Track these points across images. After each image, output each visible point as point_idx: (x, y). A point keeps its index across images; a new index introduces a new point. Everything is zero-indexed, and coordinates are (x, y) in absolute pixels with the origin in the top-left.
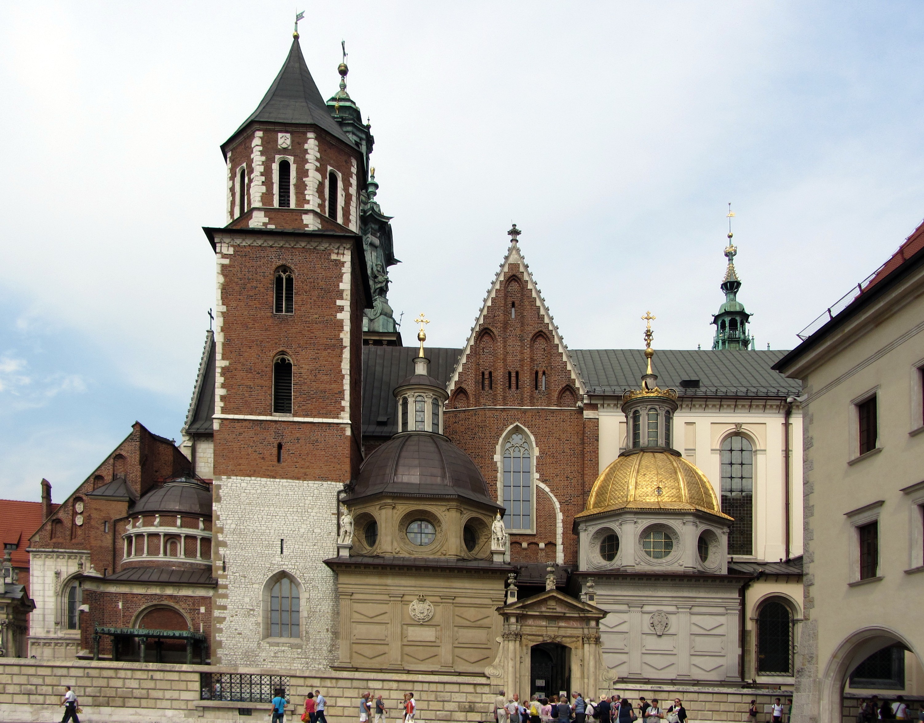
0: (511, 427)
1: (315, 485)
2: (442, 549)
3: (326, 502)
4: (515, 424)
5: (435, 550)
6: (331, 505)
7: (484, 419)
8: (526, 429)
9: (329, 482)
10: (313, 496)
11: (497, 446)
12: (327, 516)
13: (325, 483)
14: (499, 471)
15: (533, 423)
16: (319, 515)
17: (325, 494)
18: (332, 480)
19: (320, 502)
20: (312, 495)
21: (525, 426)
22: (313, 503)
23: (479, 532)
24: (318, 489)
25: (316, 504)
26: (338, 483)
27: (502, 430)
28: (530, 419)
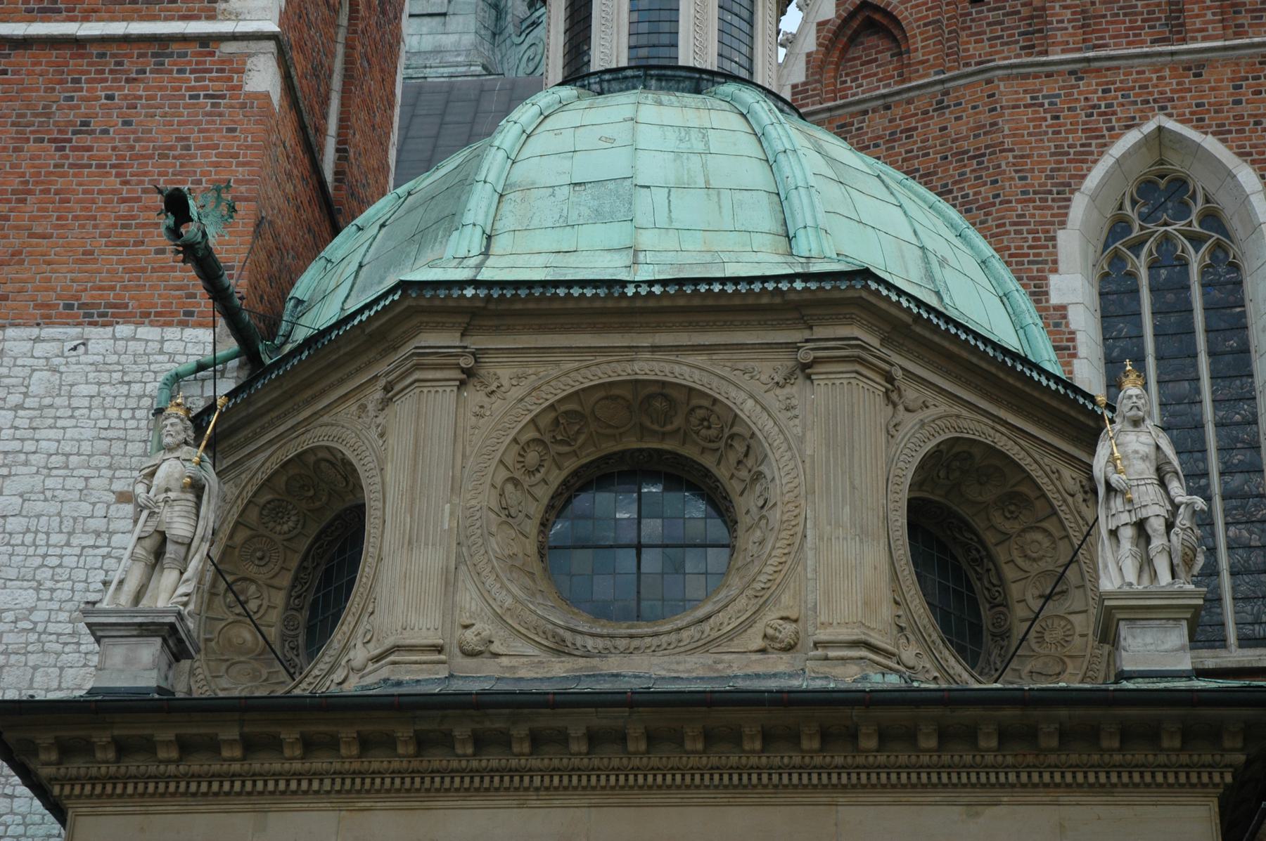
0: (1132, 138)
1: (40, 349)
2: (771, 617)
3: (94, 433)
4: (1149, 127)
5: (727, 621)
6: (117, 447)
7: (985, 118)
8: (1211, 143)
9: (123, 330)
10: (19, 407)
11: (1061, 235)
12: (85, 508)
13: (99, 338)
14: (1082, 351)
15: (1246, 109)
16: (39, 506)
17: (93, 389)
18: (145, 317)
19: (56, 434)
20: (14, 399)
21: (1200, 125)
22: (16, 445)
23: (1001, 554)
24: (55, 370)
25: (30, 446)
26: (172, 332)
27: (1085, 159)
28: (1226, 95)
